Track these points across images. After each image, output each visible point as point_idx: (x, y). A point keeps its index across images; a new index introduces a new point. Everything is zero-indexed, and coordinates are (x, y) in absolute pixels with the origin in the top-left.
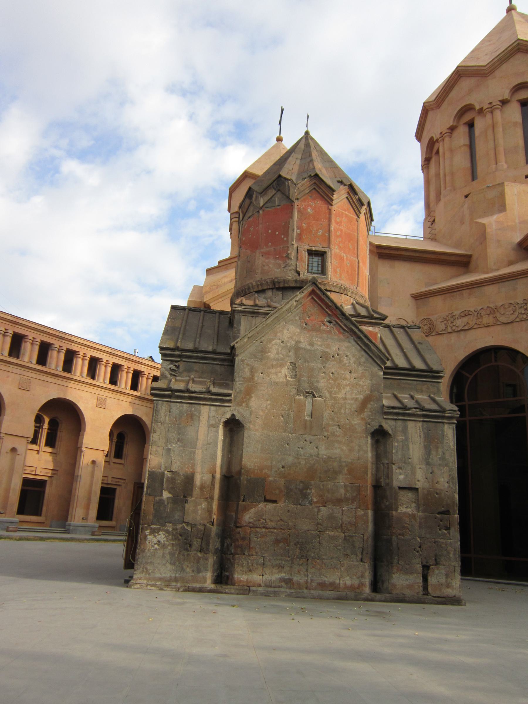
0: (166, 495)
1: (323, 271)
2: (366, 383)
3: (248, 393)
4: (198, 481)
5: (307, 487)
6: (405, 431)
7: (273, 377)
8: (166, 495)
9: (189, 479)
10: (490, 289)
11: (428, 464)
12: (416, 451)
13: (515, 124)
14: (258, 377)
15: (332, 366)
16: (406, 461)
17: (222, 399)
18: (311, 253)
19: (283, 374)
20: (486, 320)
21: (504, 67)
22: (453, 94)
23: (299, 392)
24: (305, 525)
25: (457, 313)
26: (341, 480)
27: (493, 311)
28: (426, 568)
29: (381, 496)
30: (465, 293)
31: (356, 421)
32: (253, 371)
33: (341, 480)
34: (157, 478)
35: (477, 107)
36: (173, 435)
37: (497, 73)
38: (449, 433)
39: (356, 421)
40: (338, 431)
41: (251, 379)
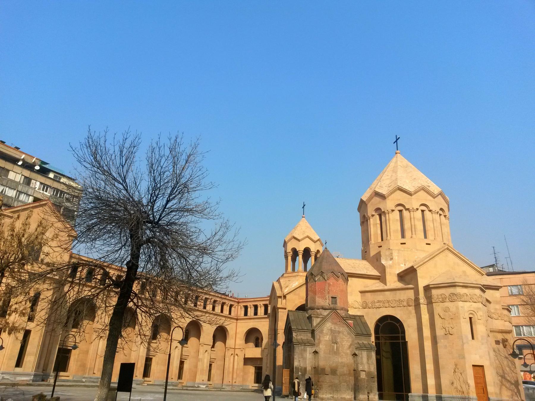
0: (300, 373)
1: (336, 303)
2: (350, 340)
3: (319, 343)
4: (308, 369)
5: (336, 371)
6: (361, 354)
7: (325, 339)
8: (300, 373)
9: (305, 369)
10: (387, 293)
11: (368, 363)
12: (365, 360)
13: (397, 220)
14: (322, 339)
15: (341, 335)
16: (362, 363)
17: (313, 345)
18: (332, 297)
19: (327, 338)
20: (387, 305)
21: (392, 195)
22: (373, 201)
23: (333, 343)
24: (337, 381)
25: (376, 301)
26: (345, 369)
27: (388, 302)
28: (368, 393)
29: (356, 373)
30: (379, 293)
31: (348, 351)
32: (320, 337)
33: (345, 369)
34: (297, 368)
35: (383, 210)
36: (300, 356)
37: (390, 197)
38: (373, 354)
39: (348, 351)
40: (344, 355)
41: (319, 339)
